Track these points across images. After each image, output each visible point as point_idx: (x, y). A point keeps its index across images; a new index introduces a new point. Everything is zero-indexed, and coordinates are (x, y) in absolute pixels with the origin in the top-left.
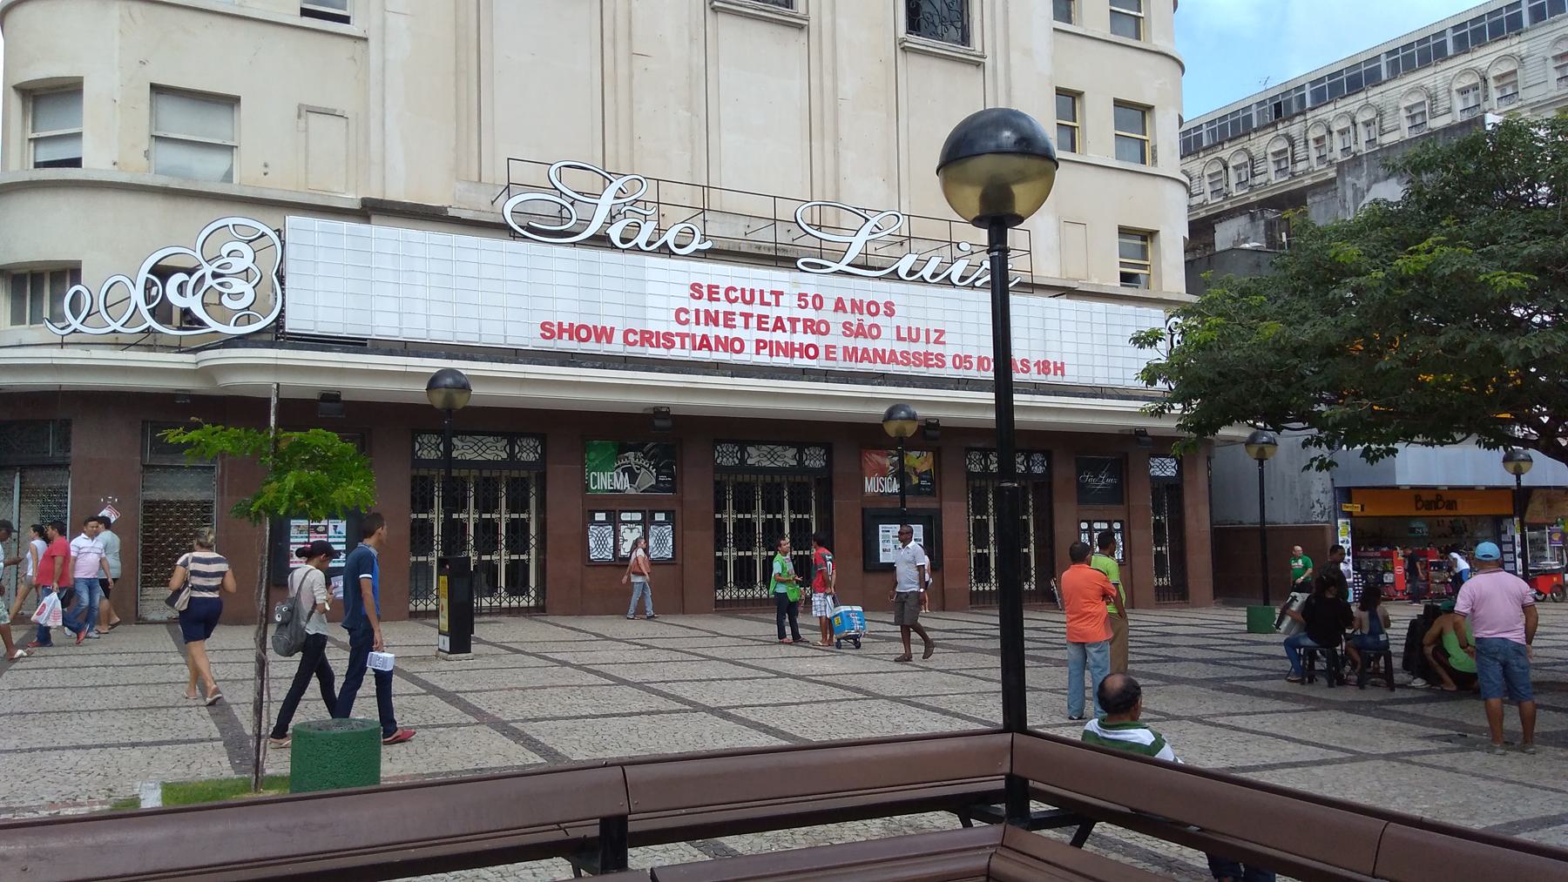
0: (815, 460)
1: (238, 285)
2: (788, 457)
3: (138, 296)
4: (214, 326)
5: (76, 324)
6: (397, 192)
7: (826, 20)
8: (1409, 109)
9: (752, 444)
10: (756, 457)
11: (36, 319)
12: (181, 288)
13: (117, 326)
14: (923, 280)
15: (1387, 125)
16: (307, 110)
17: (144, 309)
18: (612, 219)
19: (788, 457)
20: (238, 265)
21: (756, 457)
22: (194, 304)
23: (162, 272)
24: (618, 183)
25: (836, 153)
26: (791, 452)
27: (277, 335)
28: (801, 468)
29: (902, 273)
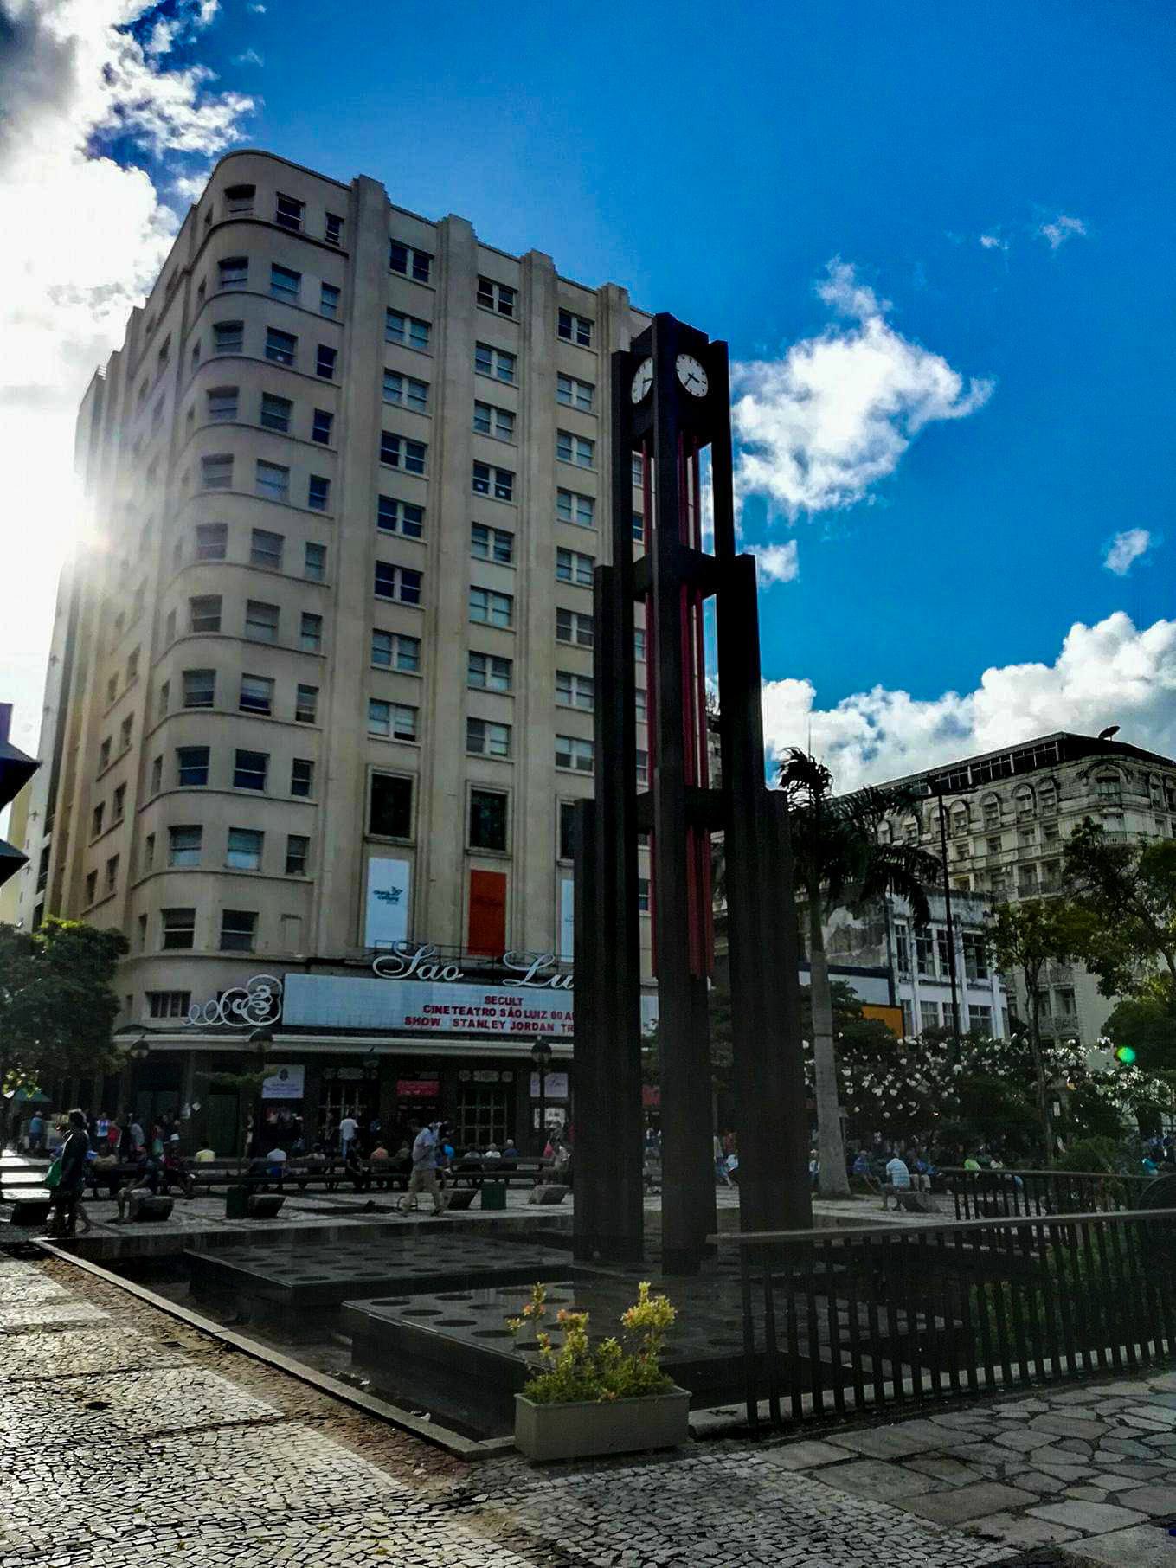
0: (508, 1077)
1: (263, 1004)
2: (494, 1077)
3: (220, 1008)
4: (252, 1022)
5: (193, 1021)
6: (322, 954)
7: (521, 855)
8: (908, 826)
9: (477, 1069)
10: (479, 1076)
11: (164, 1015)
12: (239, 1007)
13: (210, 1022)
14: (563, 988)
15: (896, 835)
16: (285, 917)
17: (222, 1015)
18: (418, 966)
19: (494, 1077)
20: (264, 995)
21: (479, 1076)
22: (244, 1012)
23: (233, 996)
24: (422, 949)
25: (523, 920)
26: (496, 1074)
27: (279, 1028)
28: (500, 1082)
29: (553, 985)
